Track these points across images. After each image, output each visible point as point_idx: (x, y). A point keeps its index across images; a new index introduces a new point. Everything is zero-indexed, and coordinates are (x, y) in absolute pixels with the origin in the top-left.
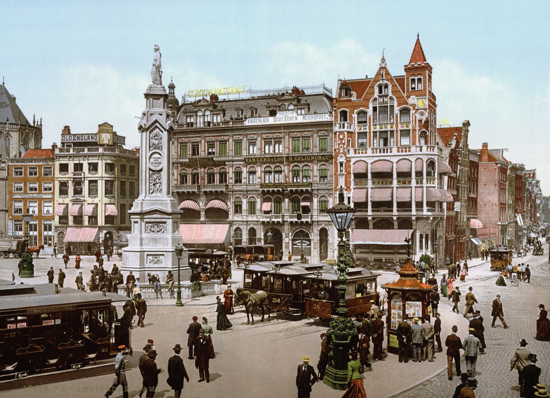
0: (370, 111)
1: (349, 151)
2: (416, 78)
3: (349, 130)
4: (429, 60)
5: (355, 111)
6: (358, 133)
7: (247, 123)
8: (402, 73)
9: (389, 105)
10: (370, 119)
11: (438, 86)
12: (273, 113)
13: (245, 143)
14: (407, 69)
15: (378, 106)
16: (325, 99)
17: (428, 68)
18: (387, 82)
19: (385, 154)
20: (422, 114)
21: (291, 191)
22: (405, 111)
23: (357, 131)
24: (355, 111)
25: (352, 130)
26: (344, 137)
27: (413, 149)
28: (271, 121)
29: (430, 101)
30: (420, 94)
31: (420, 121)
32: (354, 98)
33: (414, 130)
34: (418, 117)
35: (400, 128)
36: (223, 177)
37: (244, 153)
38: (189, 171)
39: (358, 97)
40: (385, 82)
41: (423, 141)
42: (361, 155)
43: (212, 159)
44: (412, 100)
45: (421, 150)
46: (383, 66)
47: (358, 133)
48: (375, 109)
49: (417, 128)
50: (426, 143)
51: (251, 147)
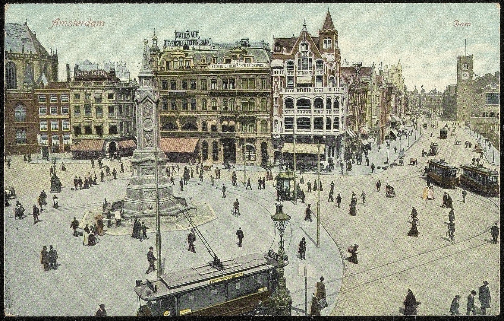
0: (296, 62)
1: (281, 89)
2: (327, 40)
3: (282, 75)
4: (337, 28)
5: (286, 62)
6: (288, 77)
7: (210, 67)
8: (317, 35)
9: (309, 58)
10: (296, 67)
11: (343, 43)
12: (228, 61)
13: (209, 82)
14: (321, 33)
15: (301, 58)
16: (265, 51)
17: (335, 33)
18: (307, 42)
19: (306, 92)
20: (331, 65)
21: (242, 116)
22: (320, 63)
23: (287, 75)
24: (286, 62)
25: (283, 75)
26: (278, 80)
27: (325, 89)
28: (228, 67)
29: (336, 56)
30: (330, 51)
31: (330, 70)
32: (284, 53)
33: (326, 76)
34: (329, 68)
35: (316, 75)
36: (194, 106)
37: (209, 89)
38: (169, 101)
39: (288, 51)
40: (306, 42)
41: (331, 83)
42: (289, 93)
43: (186, 93)
44: (324, 56)
45: (330, 91)
46: (305, 30)
47: (288, 77)
48: (299, 60)
49: (328, 75)
50: (333, 86)
51: (213, 85)
